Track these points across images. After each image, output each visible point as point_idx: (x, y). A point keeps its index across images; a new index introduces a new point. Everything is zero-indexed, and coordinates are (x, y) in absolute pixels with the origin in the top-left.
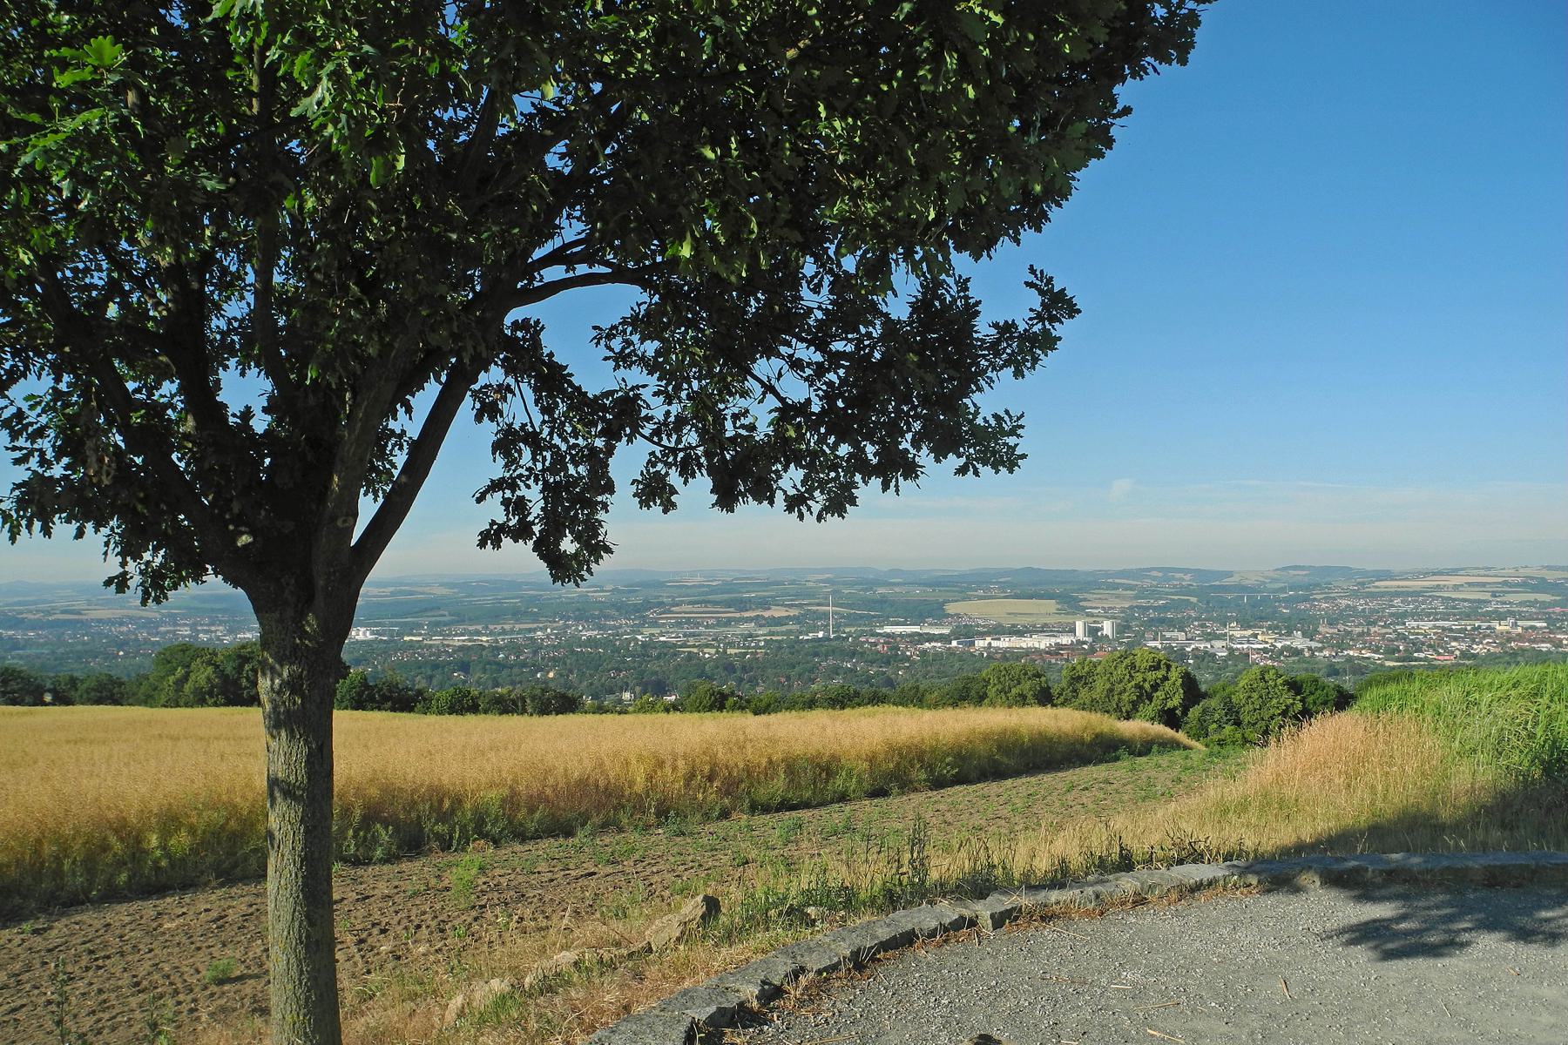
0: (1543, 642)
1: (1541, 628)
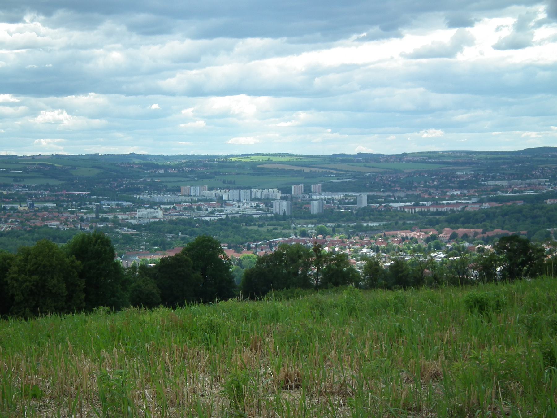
0: (53, 219)
1: (52, 208)
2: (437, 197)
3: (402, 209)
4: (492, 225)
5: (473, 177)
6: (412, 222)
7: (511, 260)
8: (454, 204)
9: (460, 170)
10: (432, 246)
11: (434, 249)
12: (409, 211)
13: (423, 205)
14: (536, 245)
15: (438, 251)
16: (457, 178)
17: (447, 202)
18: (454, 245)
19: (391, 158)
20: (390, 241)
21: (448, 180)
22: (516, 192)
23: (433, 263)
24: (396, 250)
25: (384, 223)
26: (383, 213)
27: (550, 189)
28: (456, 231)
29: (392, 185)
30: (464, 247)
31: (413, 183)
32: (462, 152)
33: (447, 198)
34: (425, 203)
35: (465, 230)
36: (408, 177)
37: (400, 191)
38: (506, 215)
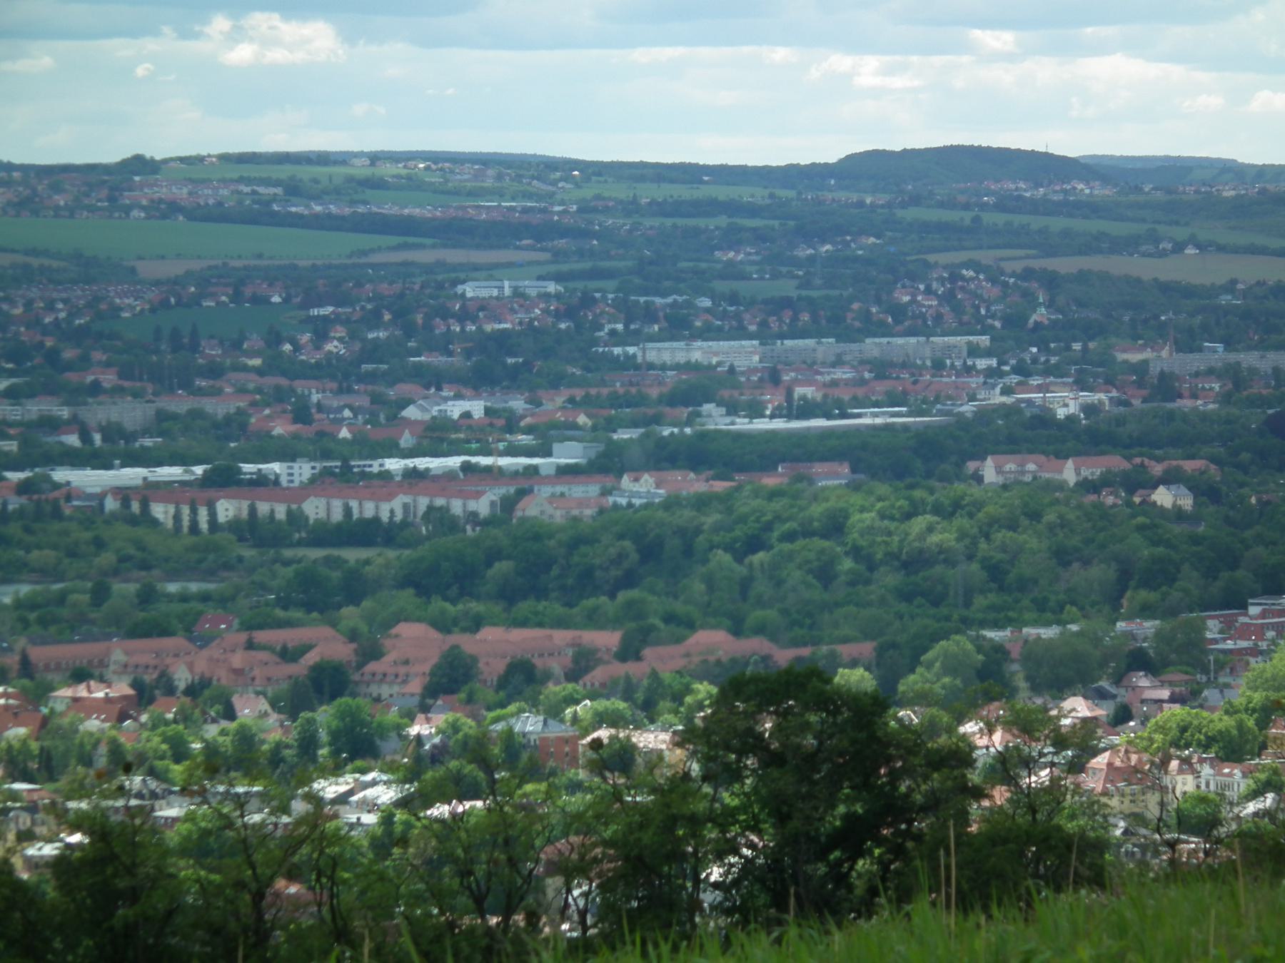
2: (344, 433)
3: (135, 507)
4: (679, 607)
5: (558, 315)
6: (194, 587)
7: (782, 819)
8: (449, 476)
9: (476, 268)
10: (323, 736)
11: (336, 753)
12: (177, 518)
13: (261, 481)
14: (932, 728)
15: (359, 763)
16: (464, 316)
17: (410, 463)
18: (455, 727)
19: (56, 188)
20: (60, 707)
21: (409, 331)
22: (807, 410)
23: (324, 840)
24: (102, 761)
25: (25, 589)
26: (14, 529)
27: (998, 399)
28: (467, 643)
29: (69, 354)
30: (512, 744)
31: (194, 347)
32: (485, 161)
33: (406, 440)
34: (276, 467)
35: (518, 634)
36: (164, 304)
37: (118, 391)
38: (755, 544)
